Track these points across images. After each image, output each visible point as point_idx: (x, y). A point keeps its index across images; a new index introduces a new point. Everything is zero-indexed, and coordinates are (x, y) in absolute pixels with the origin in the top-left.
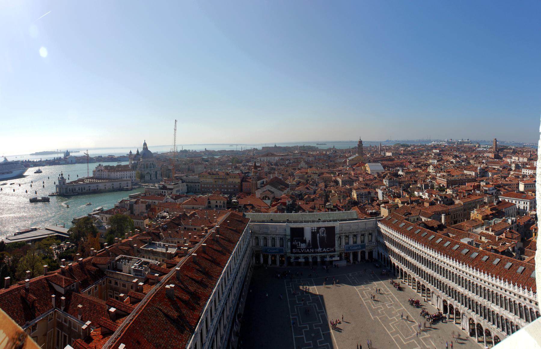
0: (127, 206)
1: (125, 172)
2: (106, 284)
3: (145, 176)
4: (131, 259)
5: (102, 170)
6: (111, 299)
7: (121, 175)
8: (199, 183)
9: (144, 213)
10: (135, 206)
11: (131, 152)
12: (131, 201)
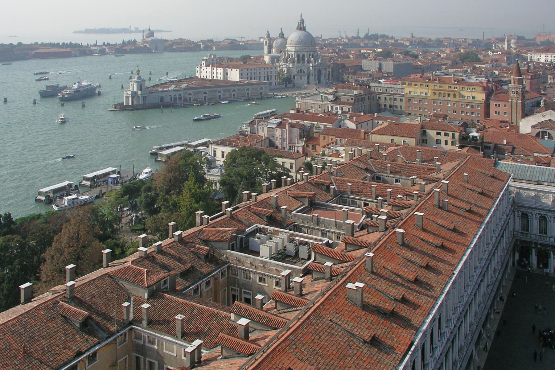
2: (227, 276)
4: (276, 233)
7: (249, 74)
8: (403, 95)
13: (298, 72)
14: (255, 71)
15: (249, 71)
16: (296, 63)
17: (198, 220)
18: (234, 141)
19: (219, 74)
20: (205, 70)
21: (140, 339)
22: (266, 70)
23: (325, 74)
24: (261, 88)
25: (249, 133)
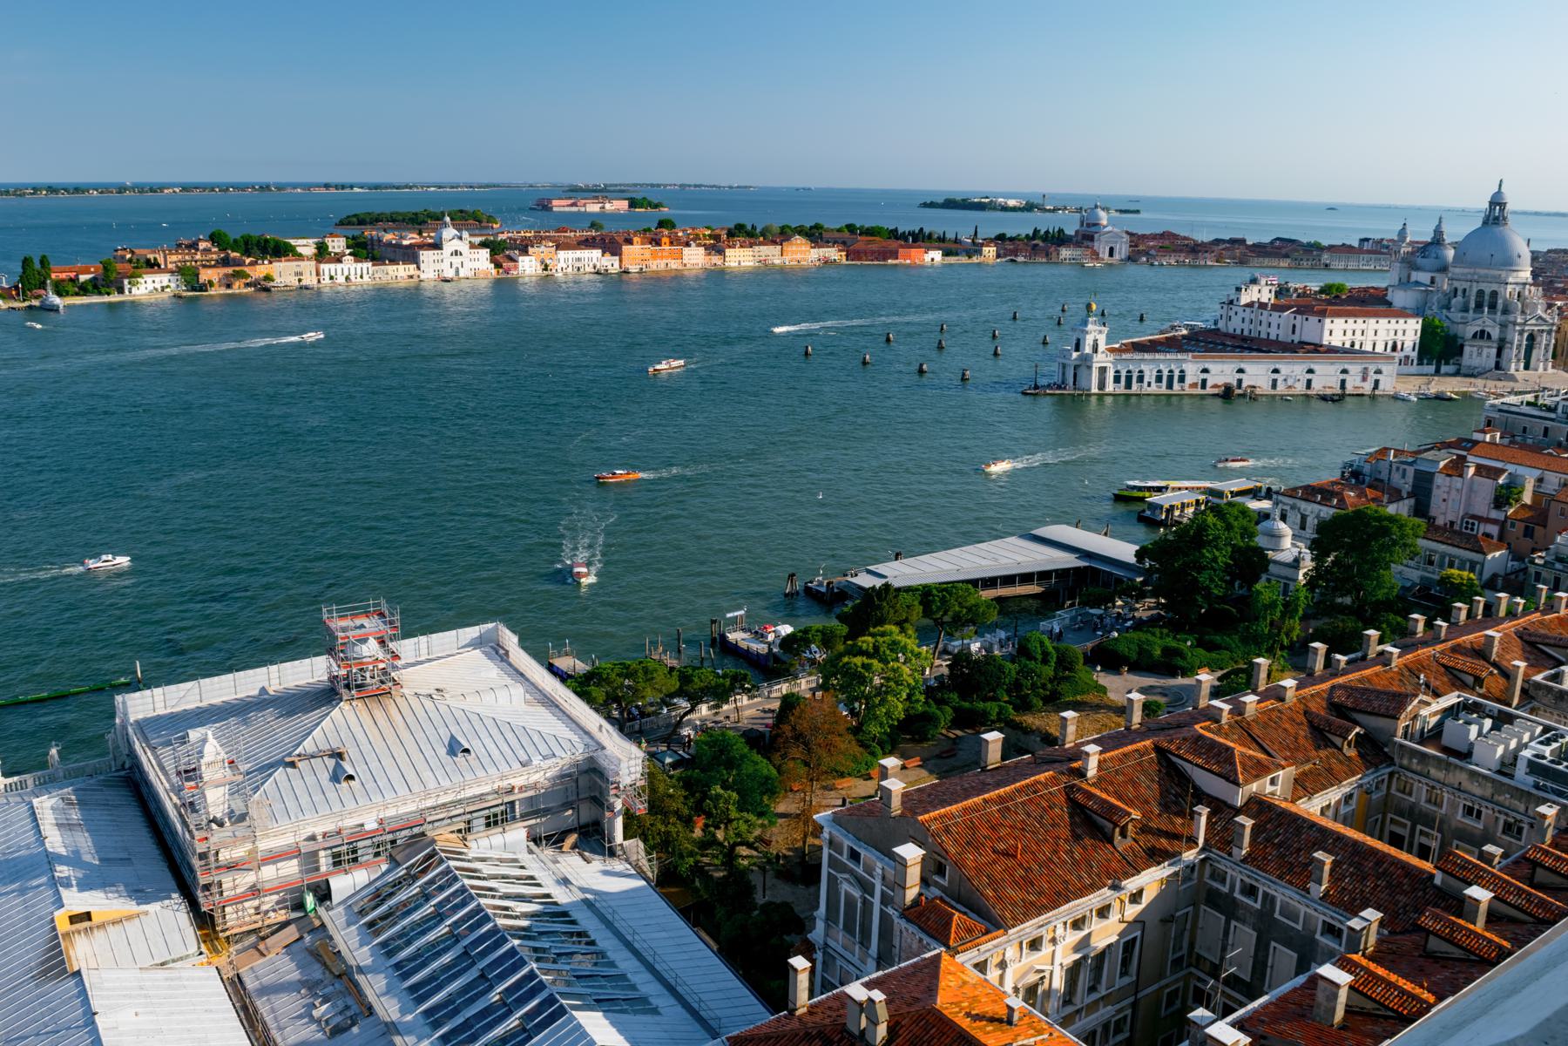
0: (1404, 476)
1: (1372, 321)
3: (1467, 349)
4: (1509, 719)
5: (1263, 306)
6: (1459, 856)
7: (1349, 333)
9: (1481, 519)
11: (1402, 233)
13: (1475, 336)
14: (1364, 326)
16: (1471, 311)
18: (1332, 494)
19: (1274, 325)
20: (1241, 314)
21: (1223, 881)
23: (1547, 345)
24: (1378, 372)
25: (1367, 479)
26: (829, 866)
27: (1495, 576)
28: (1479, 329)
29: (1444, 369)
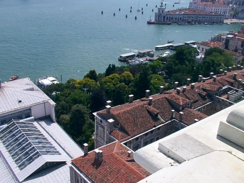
3: (239, 14)
7: (216, 10)
10: (231, 43)
12: (228, 36)
15: (216, 8)
17: (199, 79)
18: (209, 44)
20: (194, 5)
21: (177, 125)
22: (225, 8)
26: (97, 123)
27: (240, 61)
28: (242, 9)
29: (234, 17)
